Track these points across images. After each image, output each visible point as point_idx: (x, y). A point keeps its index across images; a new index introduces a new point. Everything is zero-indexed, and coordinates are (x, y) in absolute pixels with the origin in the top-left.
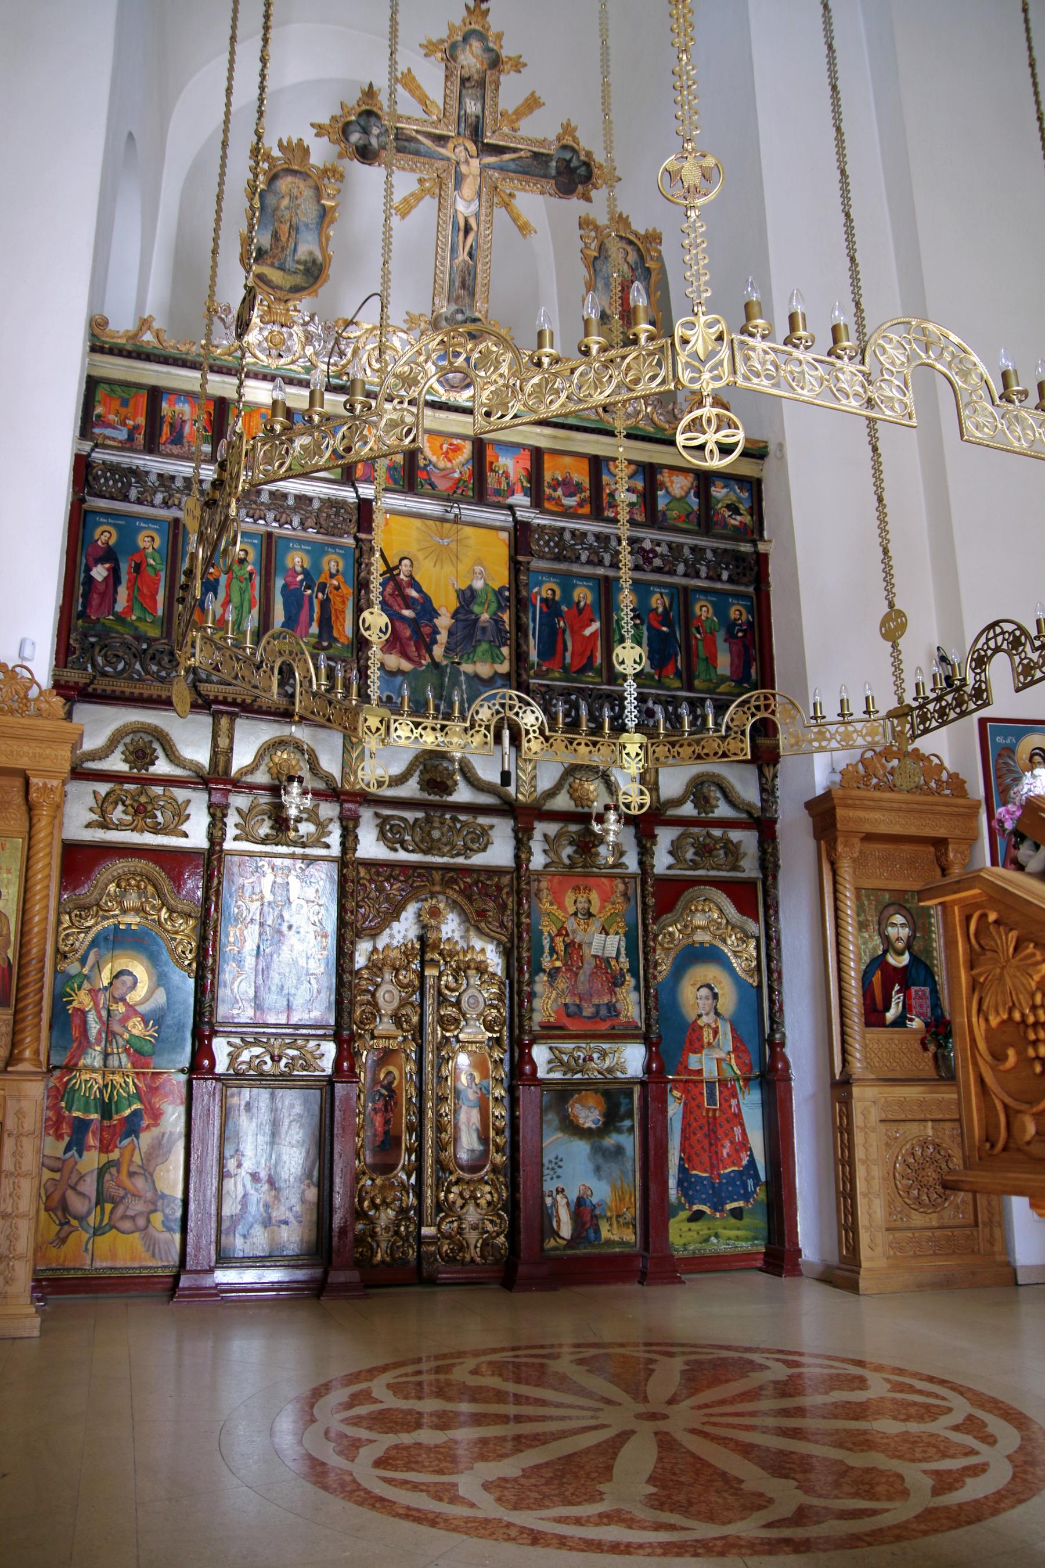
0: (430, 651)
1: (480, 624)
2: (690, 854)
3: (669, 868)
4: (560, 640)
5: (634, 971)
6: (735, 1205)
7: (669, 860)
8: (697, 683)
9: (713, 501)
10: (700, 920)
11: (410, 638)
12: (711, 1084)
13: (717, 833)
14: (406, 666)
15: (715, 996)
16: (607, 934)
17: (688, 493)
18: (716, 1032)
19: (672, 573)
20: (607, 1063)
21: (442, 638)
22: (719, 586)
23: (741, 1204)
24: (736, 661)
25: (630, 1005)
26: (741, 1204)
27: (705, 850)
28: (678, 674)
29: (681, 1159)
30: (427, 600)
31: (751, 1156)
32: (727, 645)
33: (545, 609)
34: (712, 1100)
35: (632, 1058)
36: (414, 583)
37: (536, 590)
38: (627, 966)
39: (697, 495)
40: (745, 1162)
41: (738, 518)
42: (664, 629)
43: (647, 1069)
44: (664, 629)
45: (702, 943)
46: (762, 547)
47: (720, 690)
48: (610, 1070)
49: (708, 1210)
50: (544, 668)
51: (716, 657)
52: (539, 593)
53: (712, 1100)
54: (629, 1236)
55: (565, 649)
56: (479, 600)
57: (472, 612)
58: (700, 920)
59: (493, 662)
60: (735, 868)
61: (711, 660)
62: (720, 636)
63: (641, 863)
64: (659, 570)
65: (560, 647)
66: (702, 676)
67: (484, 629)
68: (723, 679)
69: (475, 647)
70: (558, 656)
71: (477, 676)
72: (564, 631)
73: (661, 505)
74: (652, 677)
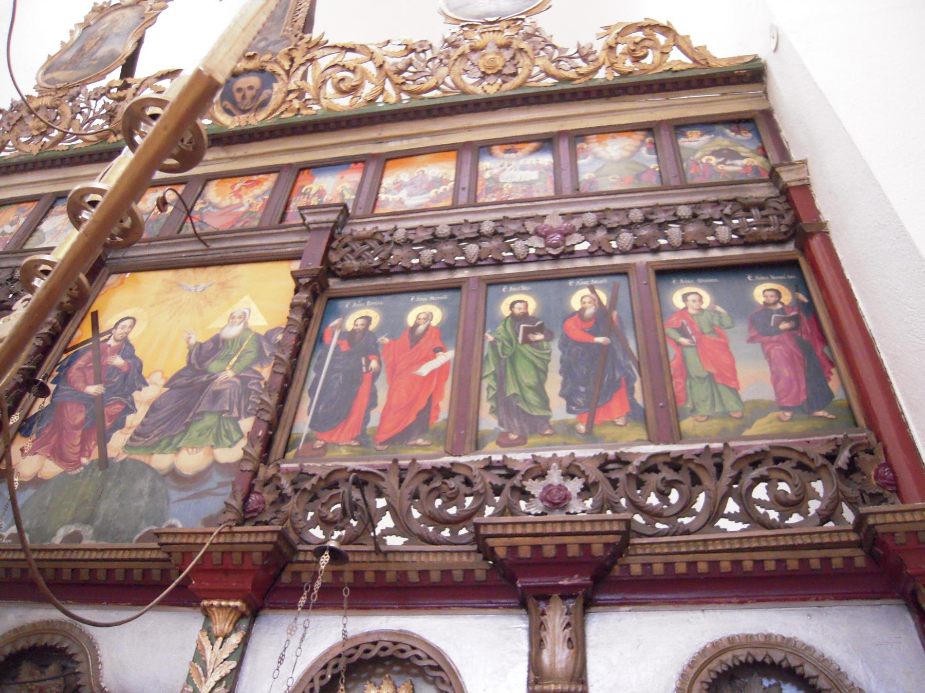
0: (104, 439)
1: (215, 387)
4: (364, 389)
8: (687, 424)
9: (683, 152)
11: (77, 427)
14: (51, 469)
21: (134, 420)
24: (786, 372)
28: (638, 415)
30: (137, 366)
32: (756, 348)
33: (345, 347)
36: (126, 349)
37: (336, 322)
41: (739, 162)
42: (600, 340)
44: (600, 340)
46: (788, 177)
47: (747, 433)
50: (319, 444)
51: (734, 371)
52: (341, 326)
55: (373, 404)
56: (222, 354)
57: (205, 372)
59: (217, 443)
61: (724, 377)
62: (738, 338)
65: (362, 400)
66: (704, 409)
67: (217, 395)
68: (758, 409)
69: (188, 425)
70: (353, 420)
71: (174, 474)
72: (375, 375)
74: (570, 428)
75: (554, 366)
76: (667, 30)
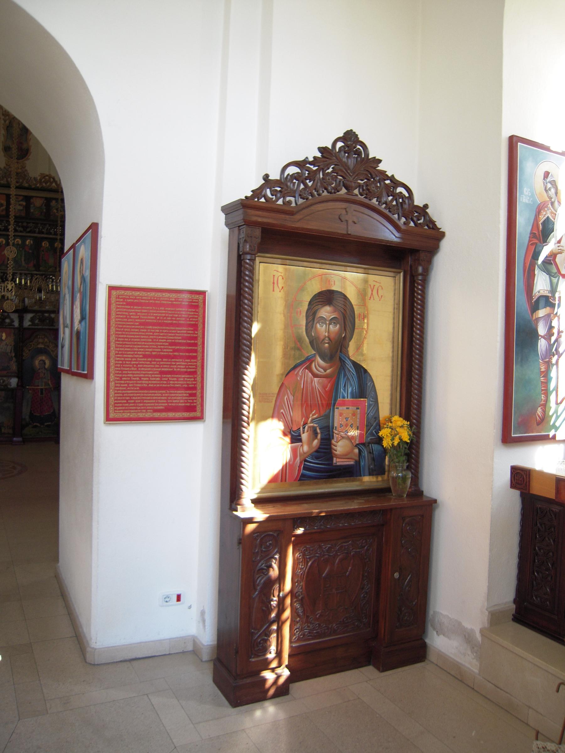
2: (37, 322)
3: (29, 325)
5: (15, 356)
6: (47, 424)
7: (30, 323)
10: (41, 340)
12: (42, 389)
13: (47, 315)
15: (45, 364)
16: (8, 345)
17: (42, 205)
18: (44, 374)
19: (34, 232)
20: (4, 384)
22: (51, 236)
23: (50, 423)
25: (14, 367)
26: (50, 423)
27: (42, 320)
29: (31, 411)
31: (54, 410)
34: (42, 393)
35: (14, 382)
38: (14, 355)
39: (45, 205)
40: (52, 411)
43: (17, 384)
45: (41, 348)
48: (6, 385)
49: (38, 424)
53: (42, 393)
54: (11, 431)
58: (41, 340)
60: (52, 325)
63: (19, 324)
64: (29, 232)
73: (32, 211)
75: (23, 255)
76: (54, 179)
